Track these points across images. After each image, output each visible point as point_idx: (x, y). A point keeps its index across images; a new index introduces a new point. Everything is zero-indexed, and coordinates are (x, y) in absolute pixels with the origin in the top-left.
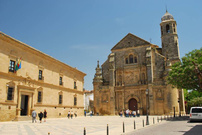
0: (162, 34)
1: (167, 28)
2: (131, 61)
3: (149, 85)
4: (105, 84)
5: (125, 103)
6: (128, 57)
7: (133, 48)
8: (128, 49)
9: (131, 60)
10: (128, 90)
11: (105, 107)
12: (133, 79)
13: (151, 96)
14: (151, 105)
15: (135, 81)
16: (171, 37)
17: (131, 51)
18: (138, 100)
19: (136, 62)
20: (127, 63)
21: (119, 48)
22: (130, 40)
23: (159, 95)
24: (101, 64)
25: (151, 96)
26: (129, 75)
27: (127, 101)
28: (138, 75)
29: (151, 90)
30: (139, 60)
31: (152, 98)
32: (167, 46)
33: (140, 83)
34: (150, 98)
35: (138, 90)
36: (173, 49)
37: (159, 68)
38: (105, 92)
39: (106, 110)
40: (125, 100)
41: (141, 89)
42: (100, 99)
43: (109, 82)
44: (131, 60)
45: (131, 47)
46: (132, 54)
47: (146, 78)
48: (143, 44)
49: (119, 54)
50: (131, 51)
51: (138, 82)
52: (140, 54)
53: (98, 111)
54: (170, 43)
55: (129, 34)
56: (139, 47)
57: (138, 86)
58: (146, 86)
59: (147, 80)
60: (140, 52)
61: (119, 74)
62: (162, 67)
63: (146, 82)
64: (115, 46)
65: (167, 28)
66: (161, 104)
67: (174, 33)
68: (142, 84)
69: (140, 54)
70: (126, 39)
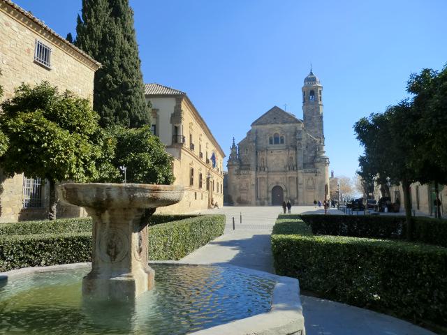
0: (304, 101)
1: (311, 94)
2: (277, 142)
3: (299, 171)
4: (243, 167)
5: (268, 192)
6: (273, 136)
7: (280, 125)
8: (274, 126)
9: (276, 140)
10: (272, 176)
11: (244, 196)
12: (278, 164)
13: (300, 184)
14: (300, 195)
15: (281, 166)
16: (316, 108)
17: (277, 128)
18: (284, 189)
19: (282, 142)
20: (271, 143)
21: (261, 124)
22: (276, 115)
23: (310, 183)
24: (236, 143)
25: (300, 184)
26: (274, 158)
27: (270, 189)
28: (285, 160)
29: (301, 177)
30: (287, 141)
31: (302, 186)
32: (310, 119)
33: (288, 168)
34: (299, 186)
35: (284, 176)
36: (318, 123)
37: (310, 152)
38: (245, 178)
39: (245, 199)
40: (268, 187)
41: (288, 176)
42: (238, 186)
43: (249, 165)
44: (276, 140)
45: (278, 123)
46: (278, 132)
47: (295, 163)
48: (293, 123)
49: (262, 132)
50: (277, 128)
51: (285, 167)
52: (288, 134)
53: (234, 198)
54: (313, 115)
55: (275, 107)
56: (287, 125)
57: (284, 171)
58: (295, 172)
59: (296, 165)
60: (287, 132)
61: (261, 157)
62: (313, 152)
63: (295, 168)
64: (256, 121)
65: (311, 94)
66: (312, 194)
67: (320, 103)
68: (289, 169)
69: (288, 134)
70: (271, 113)
